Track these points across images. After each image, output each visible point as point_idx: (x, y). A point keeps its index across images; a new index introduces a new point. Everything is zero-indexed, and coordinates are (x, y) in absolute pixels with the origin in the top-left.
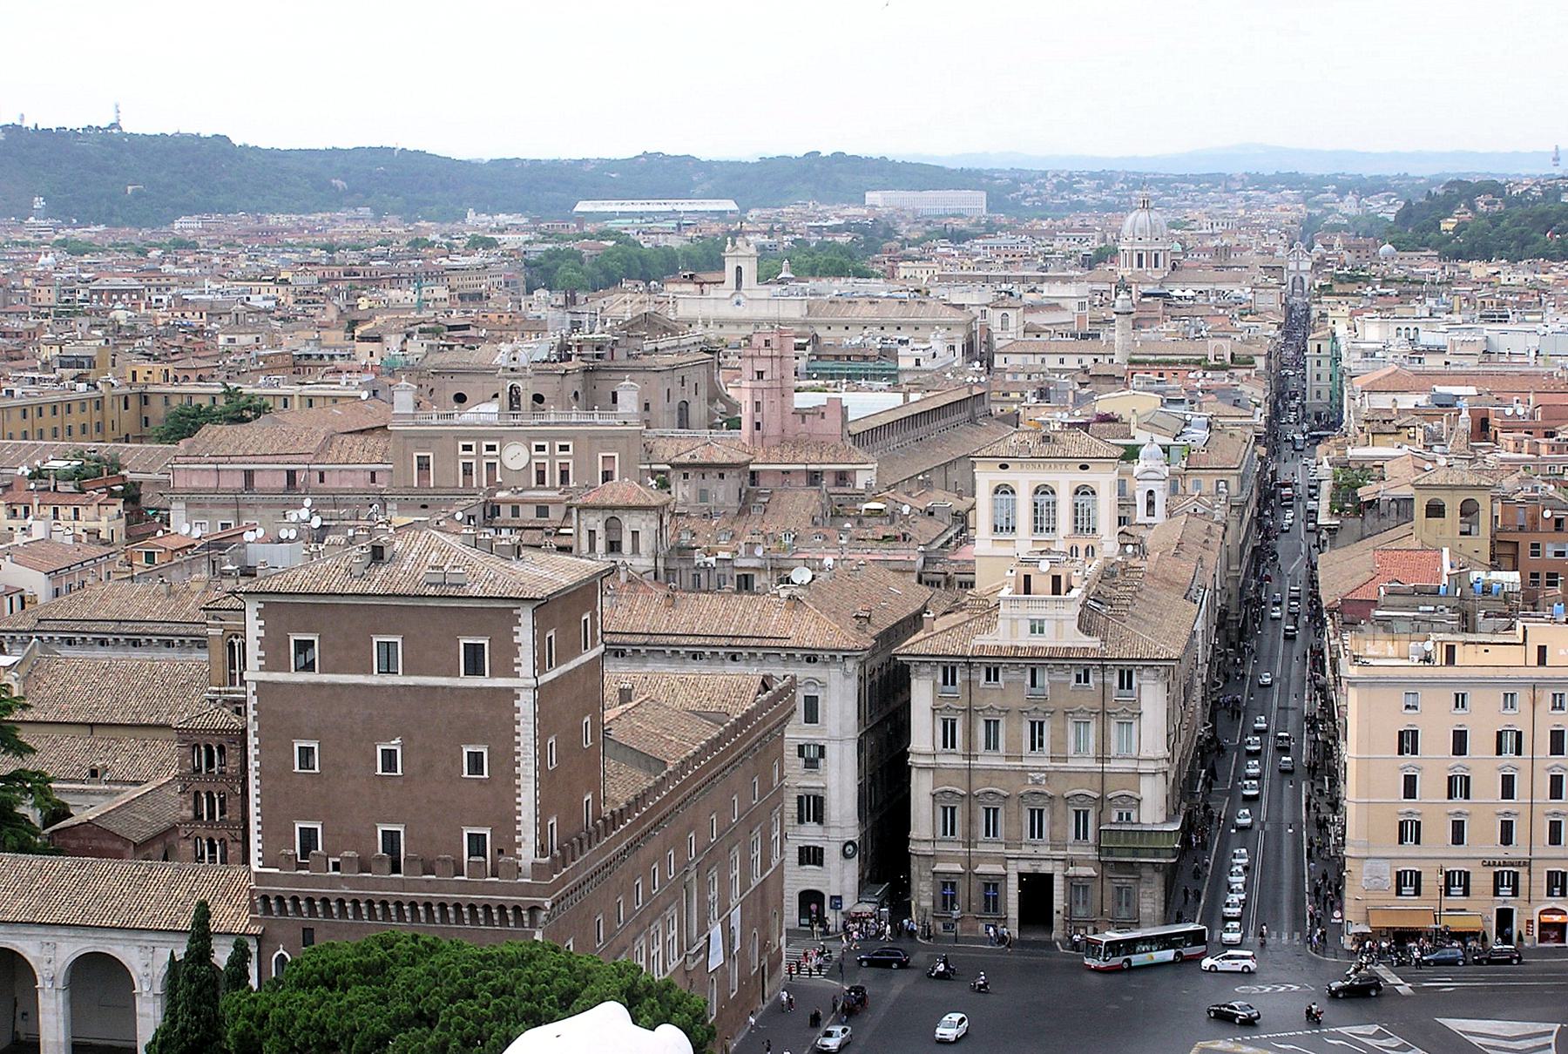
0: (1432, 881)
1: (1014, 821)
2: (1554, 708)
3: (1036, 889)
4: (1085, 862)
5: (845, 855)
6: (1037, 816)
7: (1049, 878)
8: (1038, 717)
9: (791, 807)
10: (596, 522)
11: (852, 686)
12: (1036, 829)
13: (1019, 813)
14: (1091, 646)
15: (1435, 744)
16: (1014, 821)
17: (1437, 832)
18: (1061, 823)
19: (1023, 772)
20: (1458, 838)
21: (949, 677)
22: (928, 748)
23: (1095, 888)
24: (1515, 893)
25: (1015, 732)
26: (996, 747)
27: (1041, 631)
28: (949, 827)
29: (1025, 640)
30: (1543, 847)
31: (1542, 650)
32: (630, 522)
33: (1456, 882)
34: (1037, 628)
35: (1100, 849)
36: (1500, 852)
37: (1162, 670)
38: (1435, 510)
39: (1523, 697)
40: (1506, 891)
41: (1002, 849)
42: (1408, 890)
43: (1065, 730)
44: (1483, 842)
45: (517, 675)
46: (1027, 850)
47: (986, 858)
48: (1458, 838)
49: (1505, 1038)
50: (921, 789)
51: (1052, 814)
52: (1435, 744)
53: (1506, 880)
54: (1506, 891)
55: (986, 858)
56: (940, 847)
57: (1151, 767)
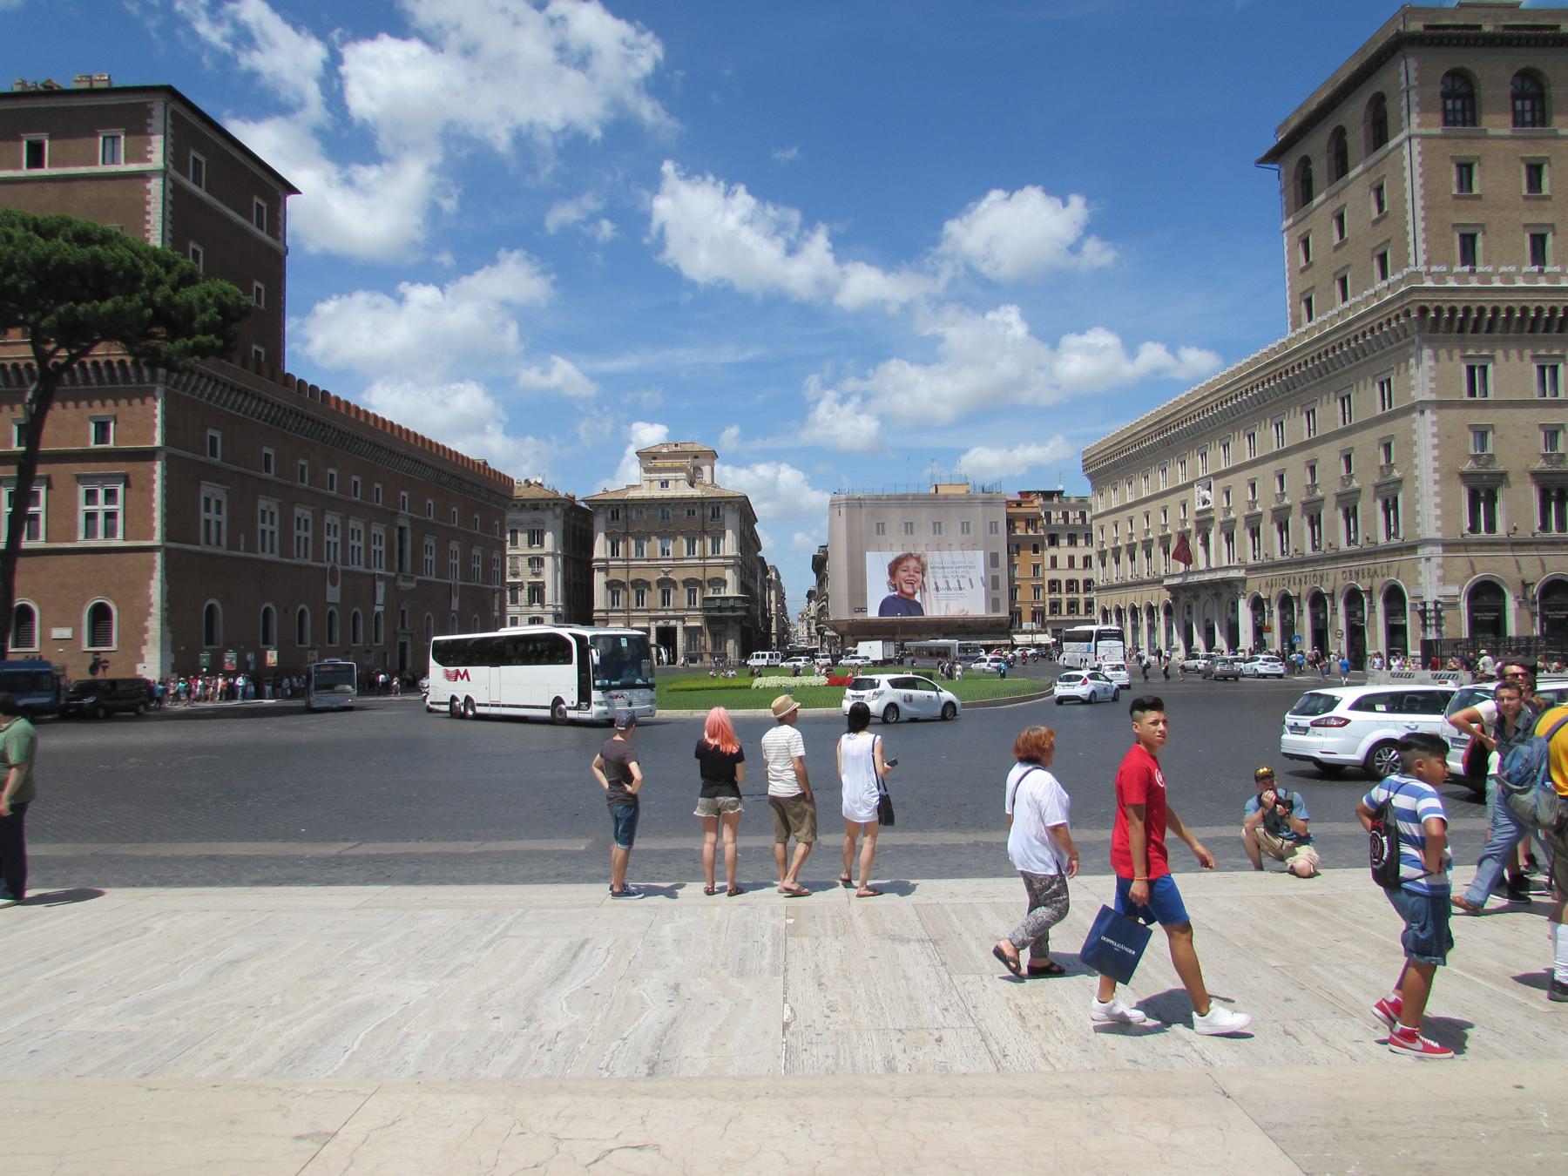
1: (653, 598)
4: (694, 618)
6: (666, 593)
9: (523, 595)
11: (559, 524)
16: (653, 598)
18: (679, 597)
19: (659, 567)
22: (603, 556)
29: (656, 492)
45: (149, 161)
50: (599, 580)
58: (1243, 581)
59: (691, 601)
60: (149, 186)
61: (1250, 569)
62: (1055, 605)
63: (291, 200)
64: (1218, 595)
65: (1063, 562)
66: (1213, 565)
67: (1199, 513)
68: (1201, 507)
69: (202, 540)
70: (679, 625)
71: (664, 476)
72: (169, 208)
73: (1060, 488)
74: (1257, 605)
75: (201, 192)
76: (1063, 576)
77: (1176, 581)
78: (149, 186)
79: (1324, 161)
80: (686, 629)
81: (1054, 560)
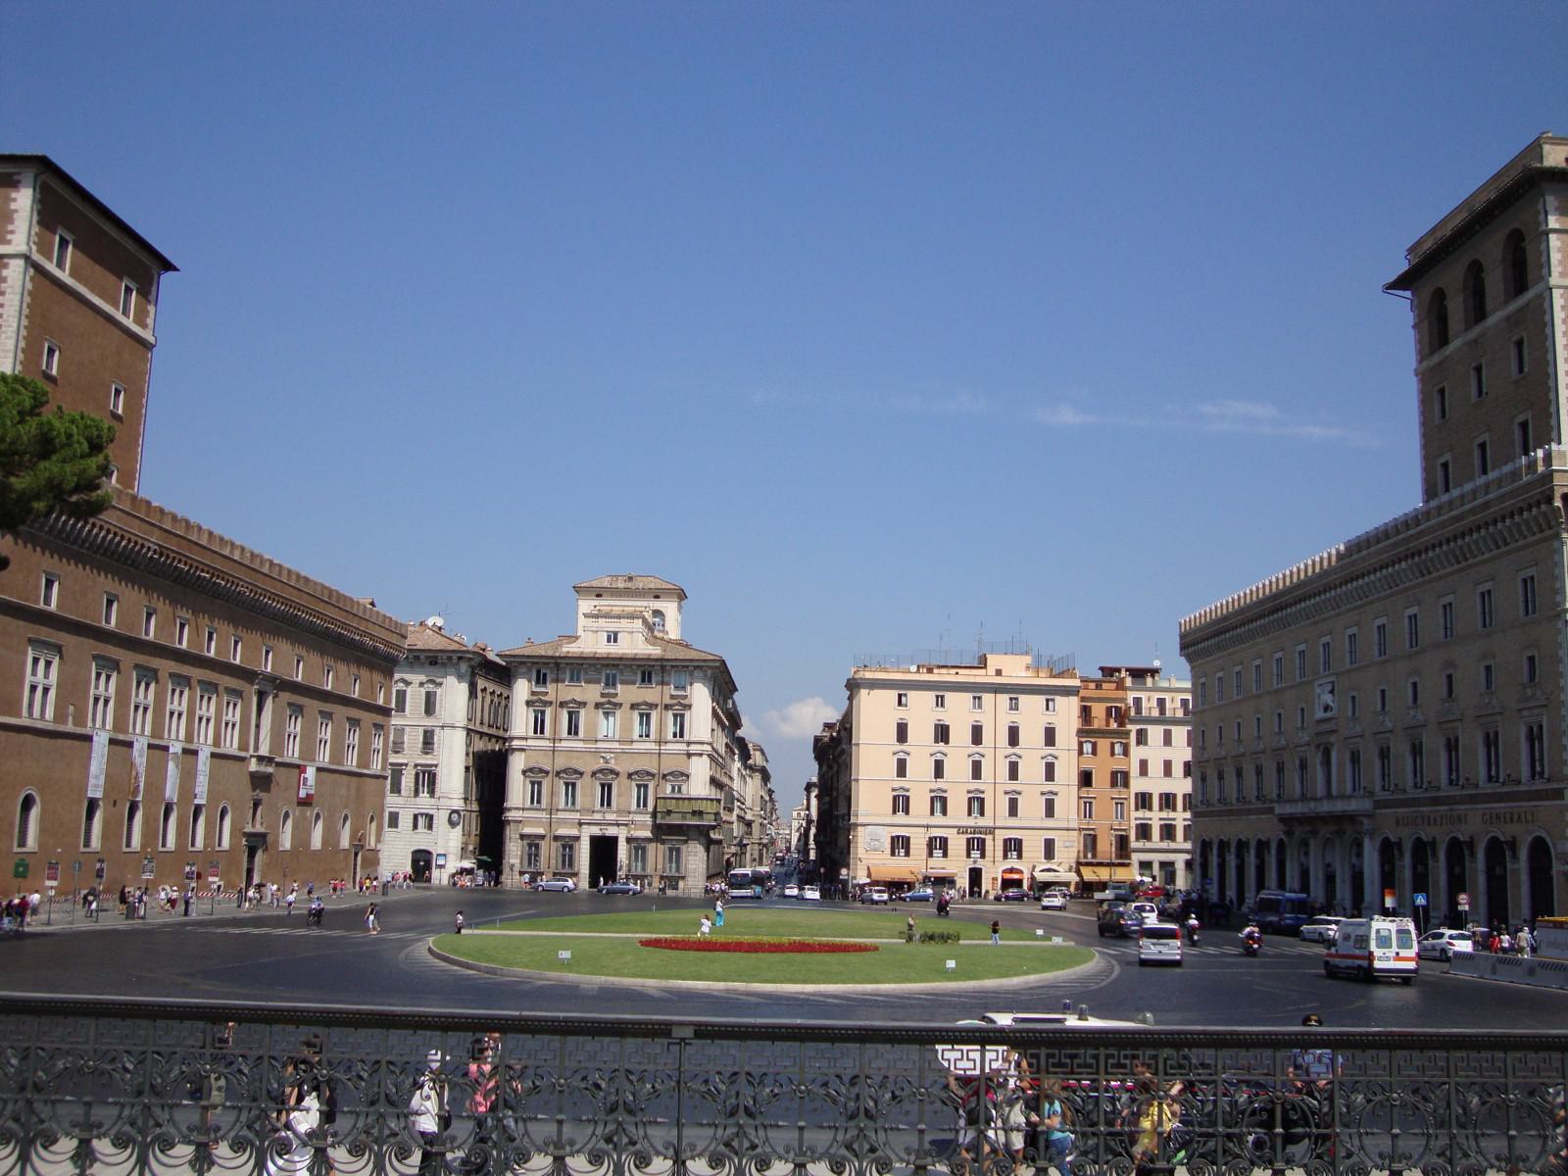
0: (919, 844)
2: (1011, 709)
3: (603, 849)
4: (642, 826)
5: (452, 824)
6: (607, 789)
7: (614, 840)
12: (606, 800)
13: (593, 787)
14: (654, 652)
16: (588, 792)
17: (920, 804)
18: (625, 794)
19: (597, 752)
21: (541, 680)
23: (651, 847)
24: (983, 856)
26: (576, 733)
27: (615, 641)
28: (536, 797)
30: (1003, 819)
31: (999, 673)
34: (613, 637)
35: (654, 814)
36: (971, 822)
37: (709, 672)
40: (975, 854)
41: (577, 816)
43: (631, 718)
46: (598, 816)
47: (564, 822)
50: (517, 764)
51: (619, 789)
52: (921, 734)
53: (975, 845)
54: (975, 854)
55: (564, 822)
56: (527, 814)
58: (1370, 816)
59: (642, 802)
60: (5, 273)
61: (1378, 805)
62: (1144, 831)
63: (167, 278)
64: (1340, 833)
65: (1156, 768)
66: (1334, 792)
67: (1319, 722)
68: (1320, 714)
69: (25, 712)
70: (622, 834)
71: (613, 625)
72: (27, 299)
73: (1156, 664)
74: (1388, 851)
75: (65, 276)
76: (1155, 785)
77: (1288, 809)
79: (1461, 298)
80: (629, 840)
81: (1144, 764)
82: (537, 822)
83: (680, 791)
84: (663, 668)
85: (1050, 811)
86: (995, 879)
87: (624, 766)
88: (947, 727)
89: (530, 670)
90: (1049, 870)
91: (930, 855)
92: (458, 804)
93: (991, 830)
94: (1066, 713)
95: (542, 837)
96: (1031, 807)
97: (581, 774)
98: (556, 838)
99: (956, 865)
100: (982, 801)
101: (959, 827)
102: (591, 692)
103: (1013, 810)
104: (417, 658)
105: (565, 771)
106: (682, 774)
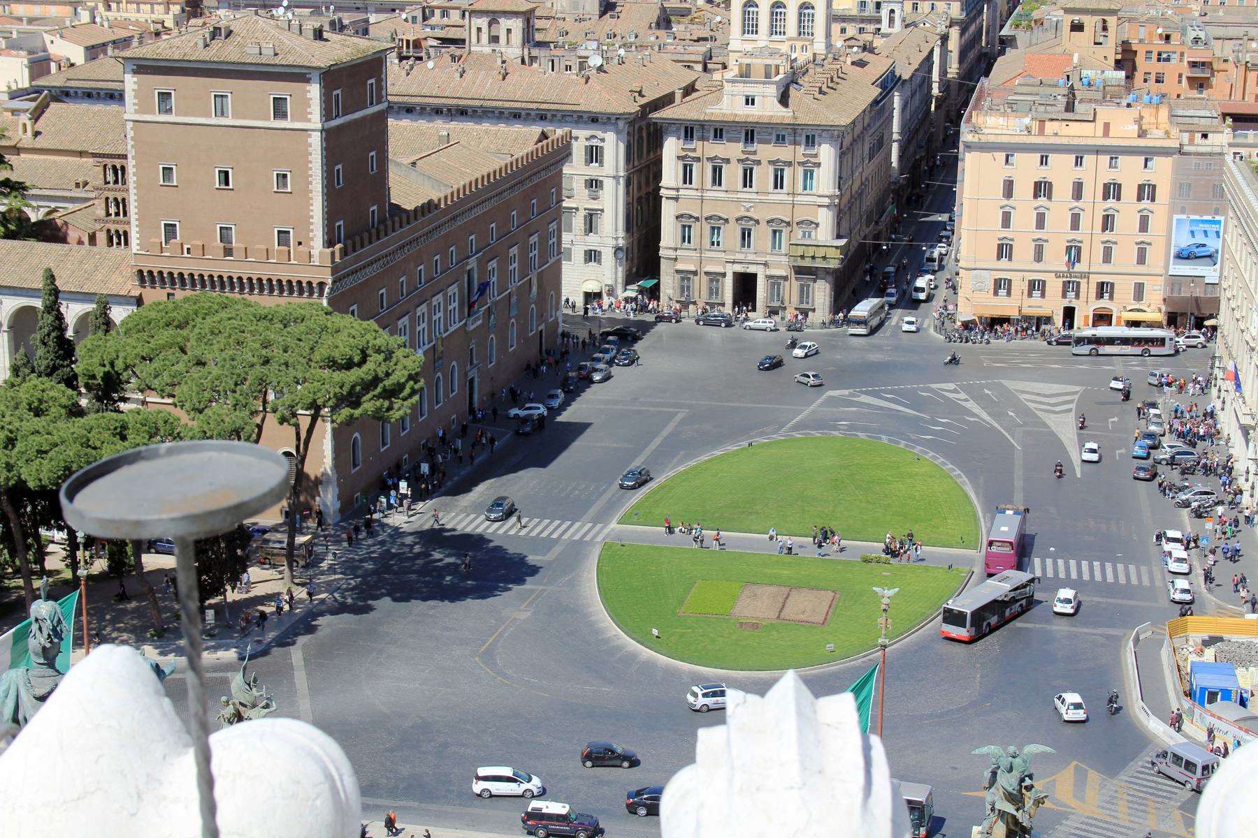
0: (1019, 286)
4: (779, 265)
6: (746, 235)
7: (755, 276)
8: (749, 164)
9: (578, 221)
10: (483, 22)
15: (1024, 190)
16: (731, 234)
18: (761, 236)
19: (738, 201)
20: (1039, 256)
22: (673, 185)
24: (1077, 296)
25: (732, 174)
26: (720, 184)
27: (753, 104)
28: (686, 238)
29: (741, 112)
30: (1098, 264)
31: (1107, 126)
32: (505, 23)
33: (1036, 286)
34: (750, 101)
38: (1077, 27)
39: (1088, 159)
40: (1071, 295)
42: (1002, 292)
44: (1056, 259)
45: (309, 121)
46: (740, 257)
48: (1039, 256)
49: (1045, 396)
50: (668, 211)
54: (1071, 295)
57: (826, 201)
60: (310, 140)
78: (310, 140)
82: (688, 260)
83: (810, 236)
84: (795, 131)
85: (1141, 260)
86: (1087, 317)
87: (762, 214)
88: (1050, 184)
89: (678, 129)
90: (1139, 310)
91: (1030, 295)
92: (621, 242)
93: (1086, 275)
94: (1162, 172)
95: (695, 273)
96: (1125, 256)
97: (727, 221)
98: (706, 273)
99: (1052, 305)
100: (1079, 250)
101: (1056, 272)
102: (733, 150)
103: (1107, 258)
104: (581, 117)
105: (710, 218)
106: (812, 222)
